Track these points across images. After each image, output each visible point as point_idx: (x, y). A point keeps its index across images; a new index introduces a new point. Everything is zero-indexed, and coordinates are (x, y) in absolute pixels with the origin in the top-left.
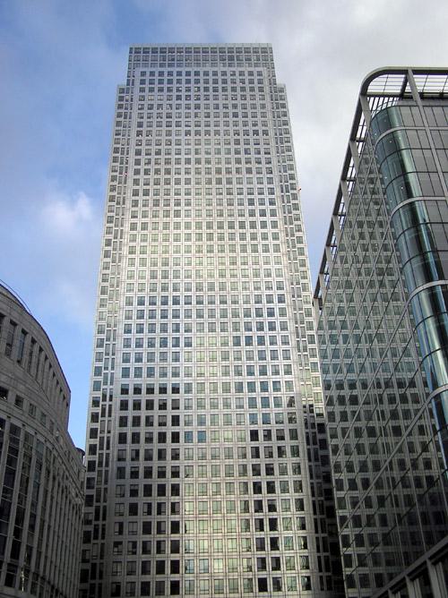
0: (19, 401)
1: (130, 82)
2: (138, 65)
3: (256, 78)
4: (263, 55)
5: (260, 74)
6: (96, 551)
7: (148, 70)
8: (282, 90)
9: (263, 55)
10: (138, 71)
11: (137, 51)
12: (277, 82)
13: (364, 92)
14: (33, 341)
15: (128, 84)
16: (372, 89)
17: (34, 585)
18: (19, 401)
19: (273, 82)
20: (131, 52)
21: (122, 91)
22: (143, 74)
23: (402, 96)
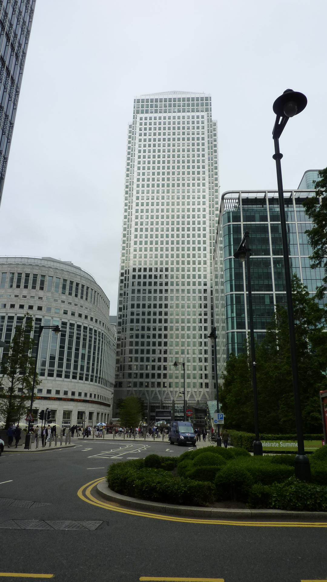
0: (92, 319)
1: (134, 123)
2: (138, 112)
4: (203, 103)
5: (203, 117)
6: (122, 360)
7: (144, 116)
8: (215, 124)
9: (203, 103)
11: (138, 101)
12: (213, 118)
13: (223, 198)
14: (95, 292)
17: (99, 381)
19: (209, 120)
20: (135, 103)
21: (130, 127)
22: (141, 119)
23: (239, 199)
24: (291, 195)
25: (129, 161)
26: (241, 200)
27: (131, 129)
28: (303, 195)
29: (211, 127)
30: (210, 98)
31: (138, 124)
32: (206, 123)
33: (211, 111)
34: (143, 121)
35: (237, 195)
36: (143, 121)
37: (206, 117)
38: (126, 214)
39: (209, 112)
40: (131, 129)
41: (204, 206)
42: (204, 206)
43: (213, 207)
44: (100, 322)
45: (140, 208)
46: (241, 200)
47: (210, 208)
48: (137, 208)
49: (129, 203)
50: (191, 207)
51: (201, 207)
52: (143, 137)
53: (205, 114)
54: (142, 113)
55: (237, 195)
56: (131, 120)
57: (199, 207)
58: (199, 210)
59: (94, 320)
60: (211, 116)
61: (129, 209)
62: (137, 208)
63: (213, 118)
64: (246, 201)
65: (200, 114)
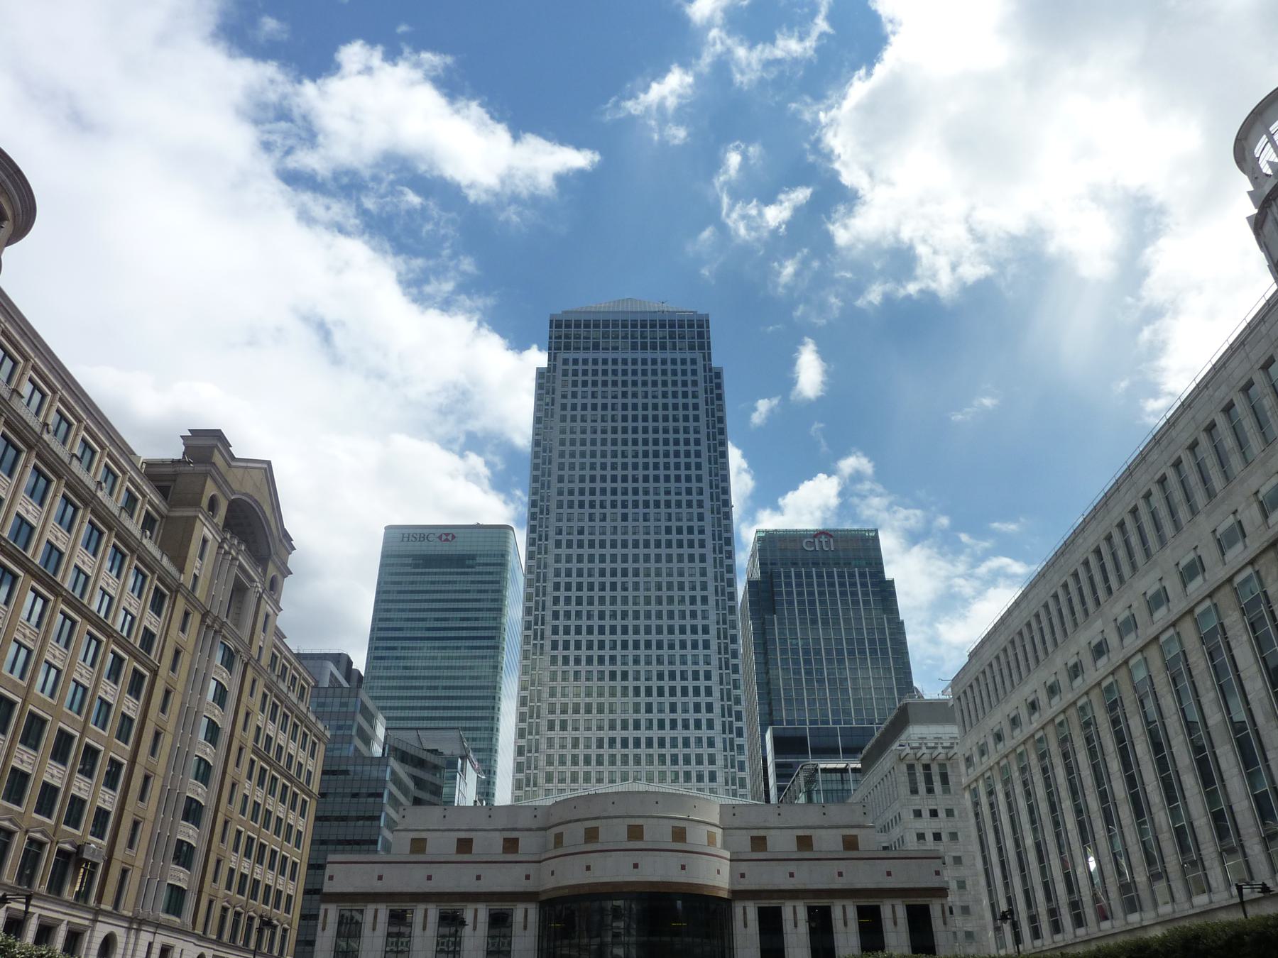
3: (689, 367)
5: (694, 362)
7: (571, 355)
8: (718, 375)
10: (562, 355)
11: (559, 325)
19: (708, 368)
22: (565, 362)
30: (708, 321)
33: (709, 348)
36: (571, 367)
37: (700, 363)
41: (702, 551)
52: (569, 401)
53: (698, 355)
54: (567, 348)
60: (710, 360)
62: (558, 551)
65: (688, 355)
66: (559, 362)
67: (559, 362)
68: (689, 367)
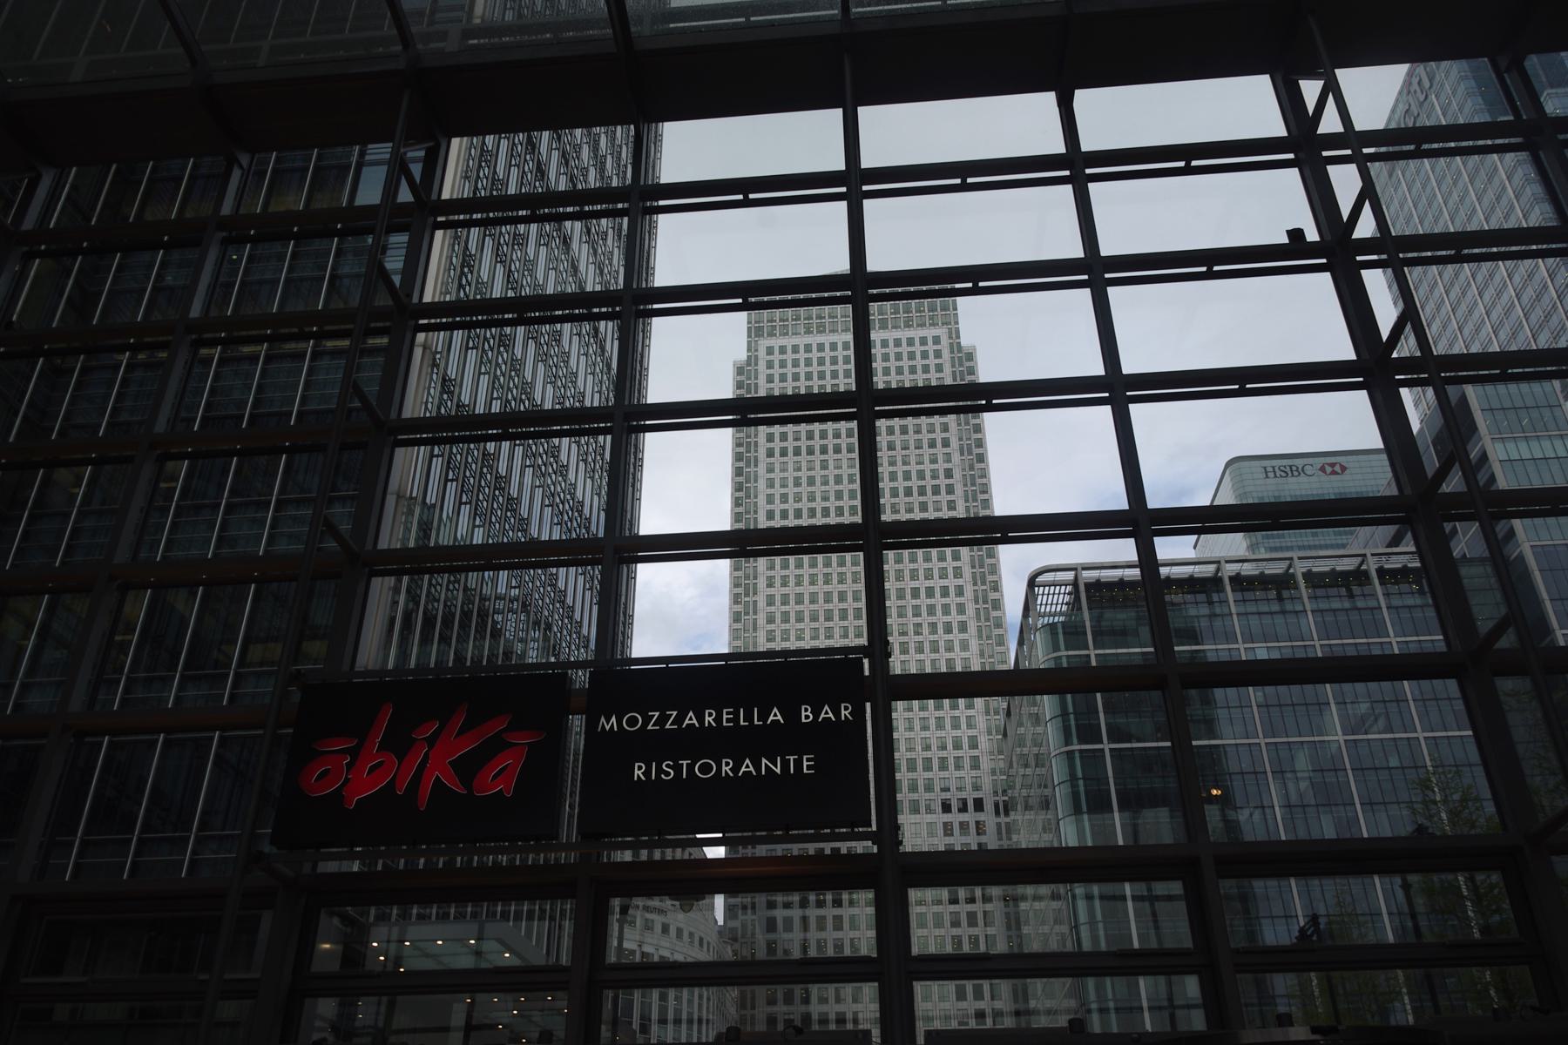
0: (679, 931)
1: (752, 360)
3: (931, 348)
5: (937, 340)
7: (776, 342)
8: (970, 356)
10: (764, 343)
12: (963, 344)
13: (1032, 583)
15: (749, 364)
16: (1040, 579)
18: (679, 931)
19: (956, 347)
21: (740, 370)
22: (770, 351)
23: (1075, 584)
24: (1218, 570)
25: (741, 464)
26: (1082, 588)
27: (743, 378)
28: (1248, 569)
29: (961, 365)
31: (762, 366)
32: (946, 354)
34: (776, 357)
35: (1070, 576)
36: (776, 357)
37: (945, 341)
38: (739, 608)
39: (953, 326)
40: (743, 378)
41: (960, 582)
42: (960, 582)
43: (983, 583)
44: (701, 940)
45: (778, 591)
46: (1082, 588)
47: (975, 584)
48: (771, 591)
49: (747, 577)
50: (922, 584)
51: (951, 582)
53: (941, 332)
54: (771, 334)
55: (1070, 576)
56: (742, 355)
57: (944, 582)
58: (945, 592)
59: (686, 934)
61: (747, 595)
62: (771, 591)
63: (965, 341)
64: (1095, 587)
65: (929, 333)
66: (762, 353)
67: (762, 353)
68: (931, 348)
